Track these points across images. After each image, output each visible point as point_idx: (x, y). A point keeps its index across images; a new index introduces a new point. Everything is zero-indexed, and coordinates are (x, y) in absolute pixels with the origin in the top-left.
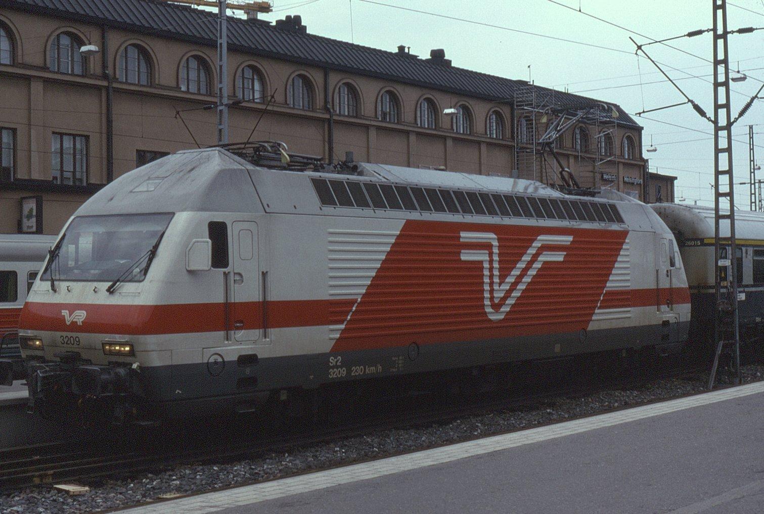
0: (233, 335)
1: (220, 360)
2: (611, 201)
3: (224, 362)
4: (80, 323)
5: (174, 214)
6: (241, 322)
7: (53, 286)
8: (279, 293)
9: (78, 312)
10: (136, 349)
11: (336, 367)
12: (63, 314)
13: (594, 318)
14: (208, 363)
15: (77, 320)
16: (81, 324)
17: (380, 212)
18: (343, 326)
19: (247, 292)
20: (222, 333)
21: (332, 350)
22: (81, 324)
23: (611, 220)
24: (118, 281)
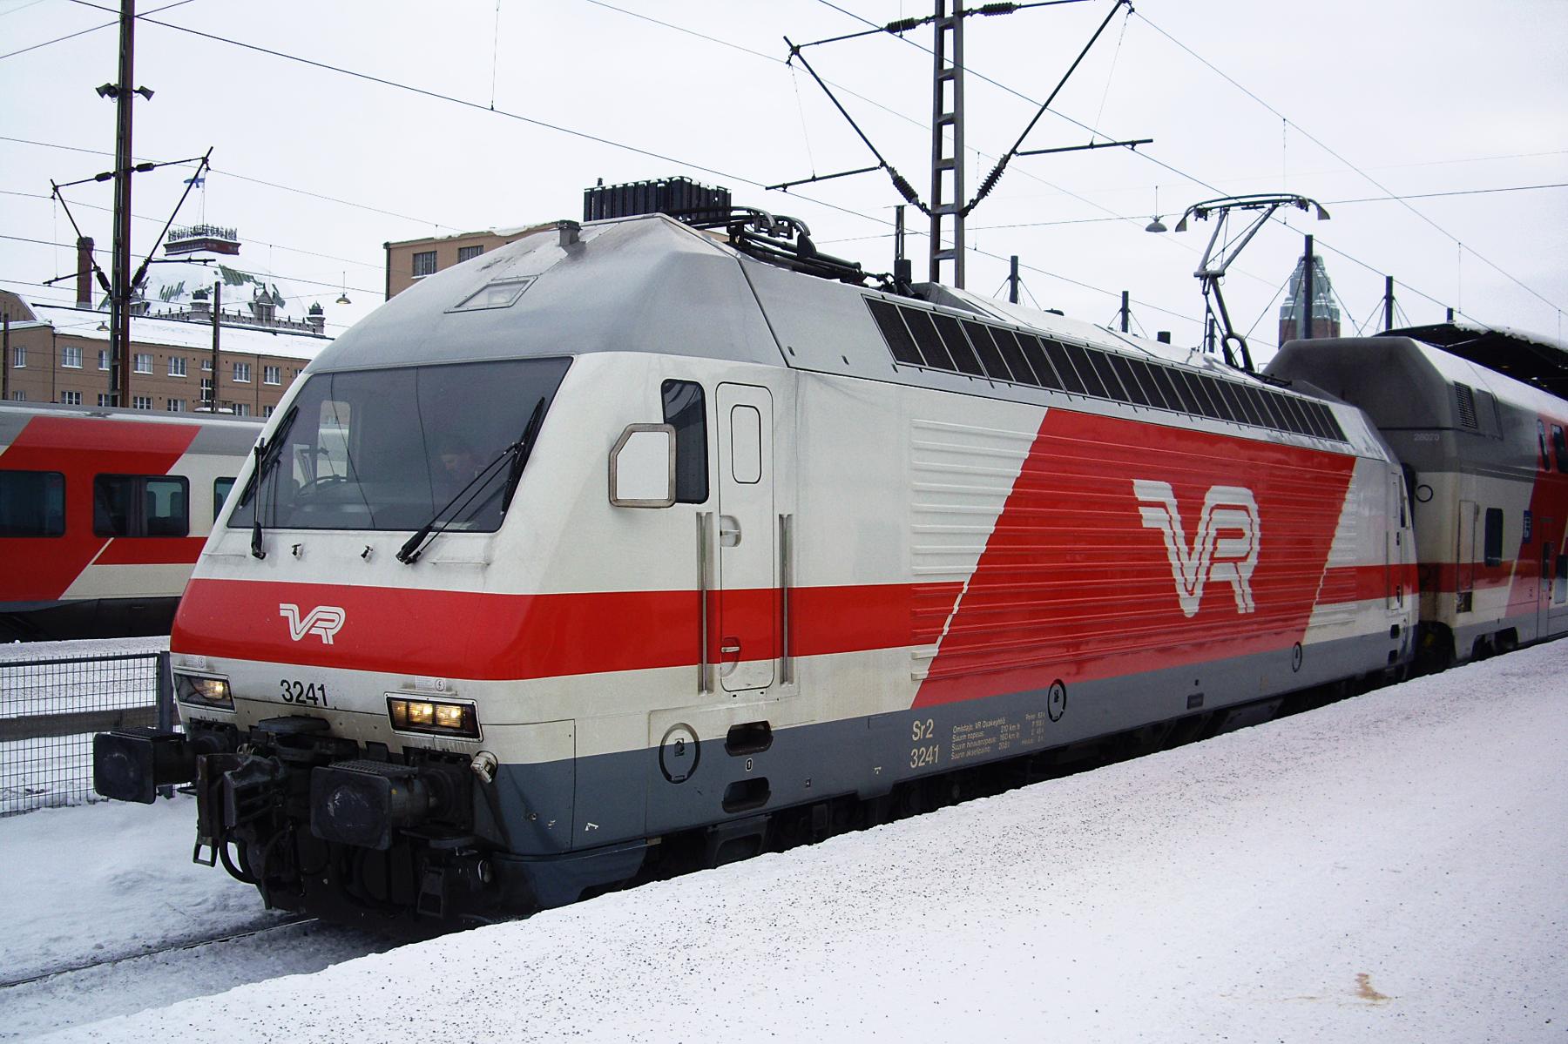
0: (717, 677)
1: (688, 739)
2: (1323, 402)
3: (697, 743)
4: (328, 639)
6: (735, 642)
7: (257, 543)
8: (819, 569)
9: (321, 611)
10: (481, 718)
11: (924, 742)
12: (283, 613)
14: (662, 747)
15: (321, 632)
17: (1001, 387)
18: (932, 650)
19: (746, 569)
20: (693, 669)
23: (1331, 437)
24: (429, 528)
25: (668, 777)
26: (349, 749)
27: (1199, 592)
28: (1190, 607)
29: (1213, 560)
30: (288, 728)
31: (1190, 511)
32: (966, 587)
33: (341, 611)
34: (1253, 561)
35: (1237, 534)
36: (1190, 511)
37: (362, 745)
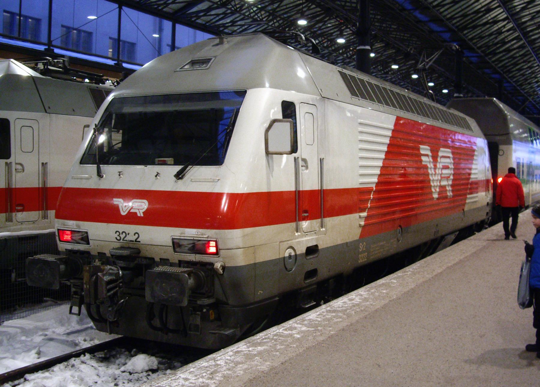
1: (293, 254)
4: (140, 214)
5: (246, 92)
6: (306, 212)
13: (467, 201)
15: (137, 211)
16: (142, 215)
18: (364, 214)
20: (293, 224)
21: (362, 236)
22: (142, 215)
25: (286, 269)
26: (151, 262)
27: (438, 190)
28: (436, 196)
29: (441, 177)
30: (125, 252)
31: (435, 158)
32: (374, 188)
33: (146, 202)
34: (452, 177)
35: (446, 167)
36: (435, 158)
37: (157, 259)
